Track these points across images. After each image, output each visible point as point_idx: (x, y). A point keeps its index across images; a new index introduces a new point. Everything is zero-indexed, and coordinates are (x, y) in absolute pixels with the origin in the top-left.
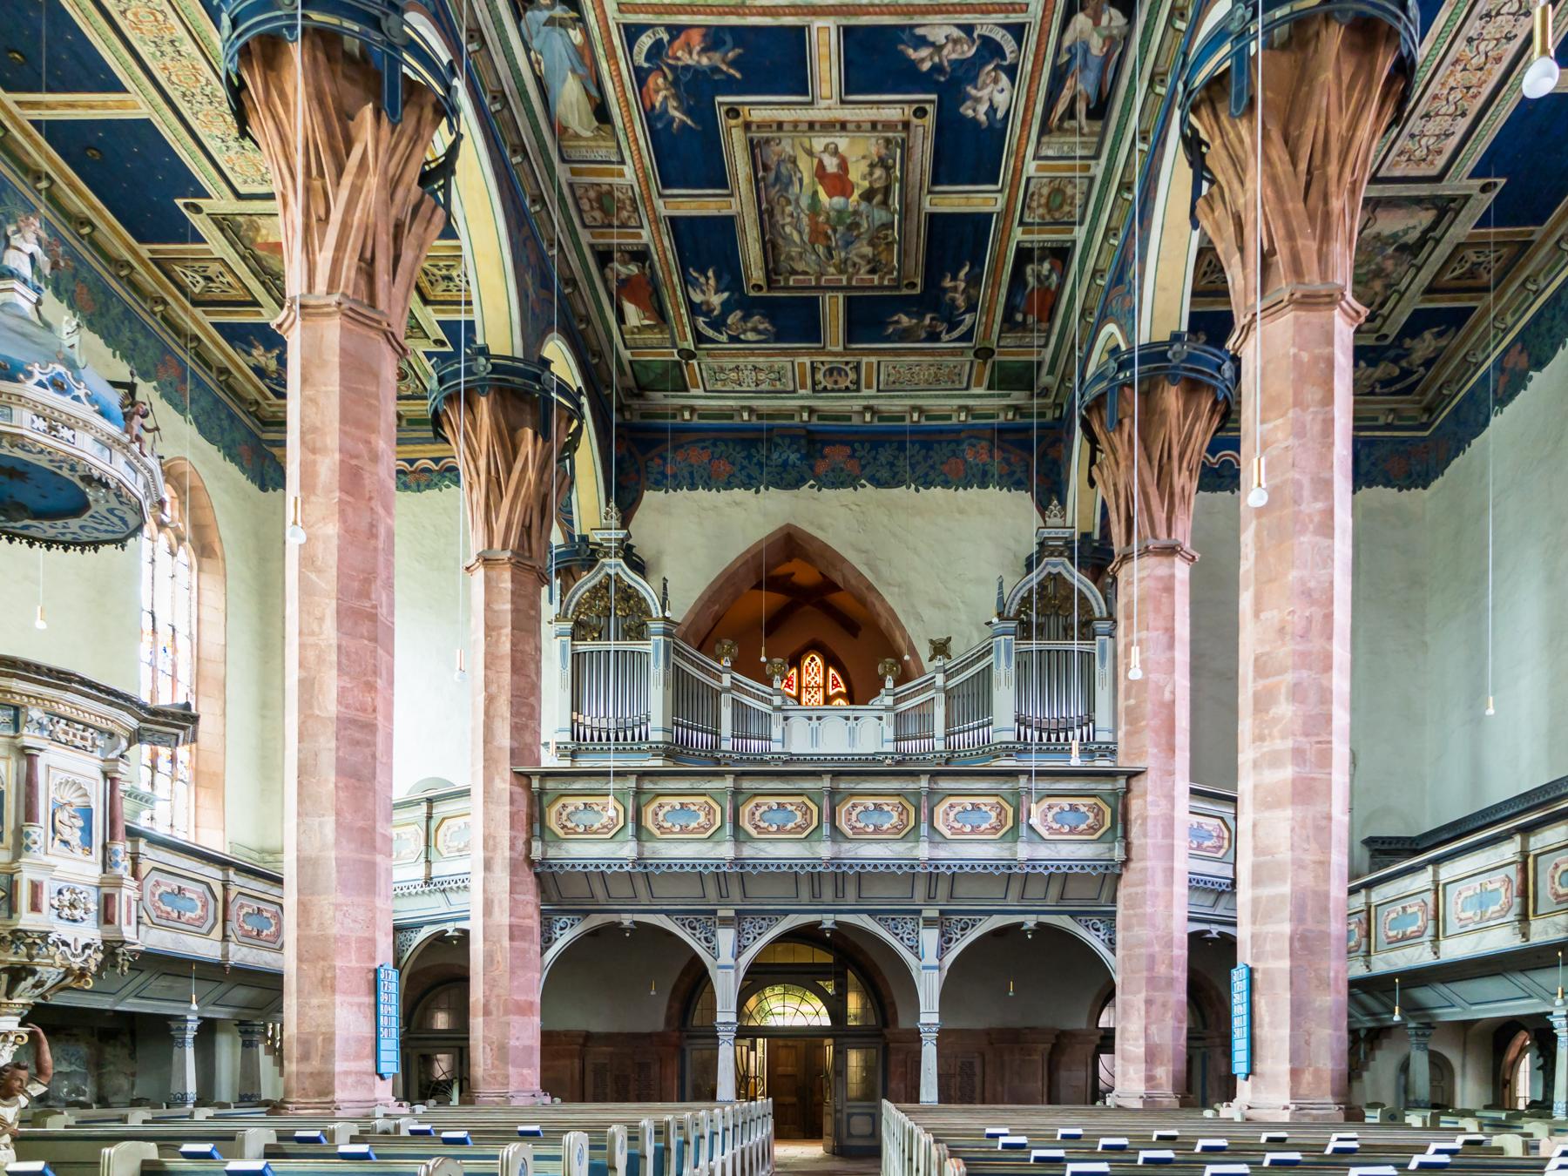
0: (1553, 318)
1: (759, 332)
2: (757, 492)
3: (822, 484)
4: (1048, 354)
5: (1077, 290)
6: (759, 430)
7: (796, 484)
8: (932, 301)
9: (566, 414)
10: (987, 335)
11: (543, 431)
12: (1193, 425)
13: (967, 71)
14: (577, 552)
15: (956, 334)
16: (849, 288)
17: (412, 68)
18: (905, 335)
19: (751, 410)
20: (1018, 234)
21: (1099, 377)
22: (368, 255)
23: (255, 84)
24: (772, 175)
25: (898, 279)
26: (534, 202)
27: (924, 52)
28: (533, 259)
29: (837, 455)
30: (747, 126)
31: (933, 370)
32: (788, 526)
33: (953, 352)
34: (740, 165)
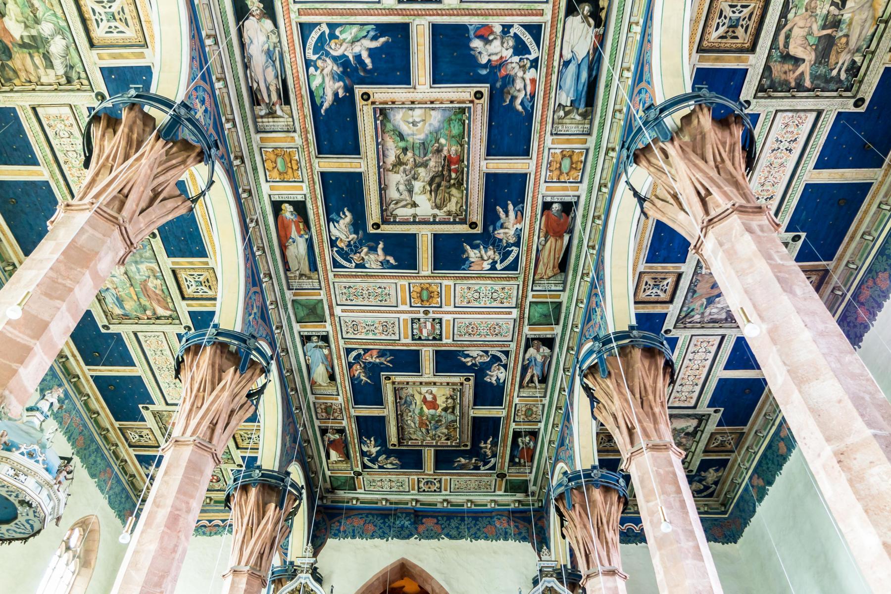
0: (767, 464)
1: (393, 464)
2: (387, 540)
3: (421, 537)
4: (532, 476)
5: (544, 451)
6: (391, 510)
7: (408, 537)
8: (475, 452)
9: (294, 497)
10: (502, 468)
11: (280, 504)
12: (610, 508)
14: (286, 571)
15: (487, 467)
16: (436, 446)
17: (255, 356)
18: (462, 467)
19: (387, 500)
20: (513, 426)
21: (560, 485)
22: (215, 421)
23: (188, 359)
24: (403, 401)
25: (460, 443)
26: (297, 409)
27: (468, 359)
28: (291, 431)
29: (429, 523)
30: (394, 383)
31: (477, 483)
32: (403, 559)
33: (486, 475)
34: (389, 396)
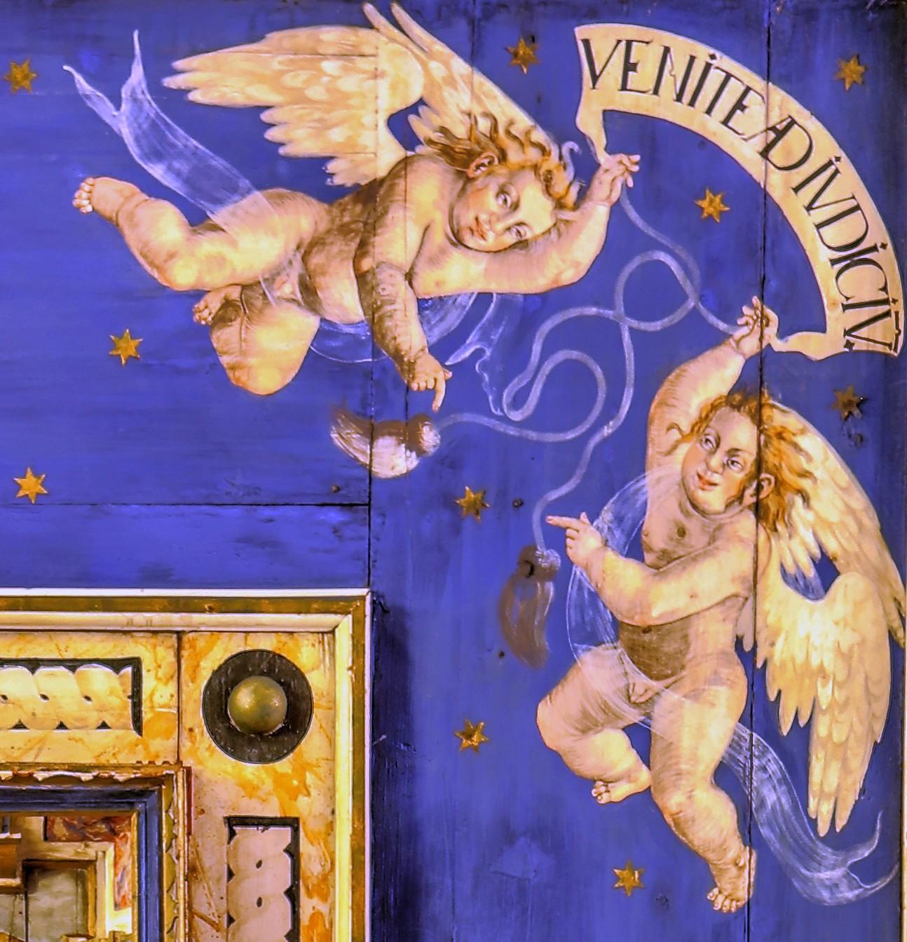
13: (569, 395)
27: (258, 237)
